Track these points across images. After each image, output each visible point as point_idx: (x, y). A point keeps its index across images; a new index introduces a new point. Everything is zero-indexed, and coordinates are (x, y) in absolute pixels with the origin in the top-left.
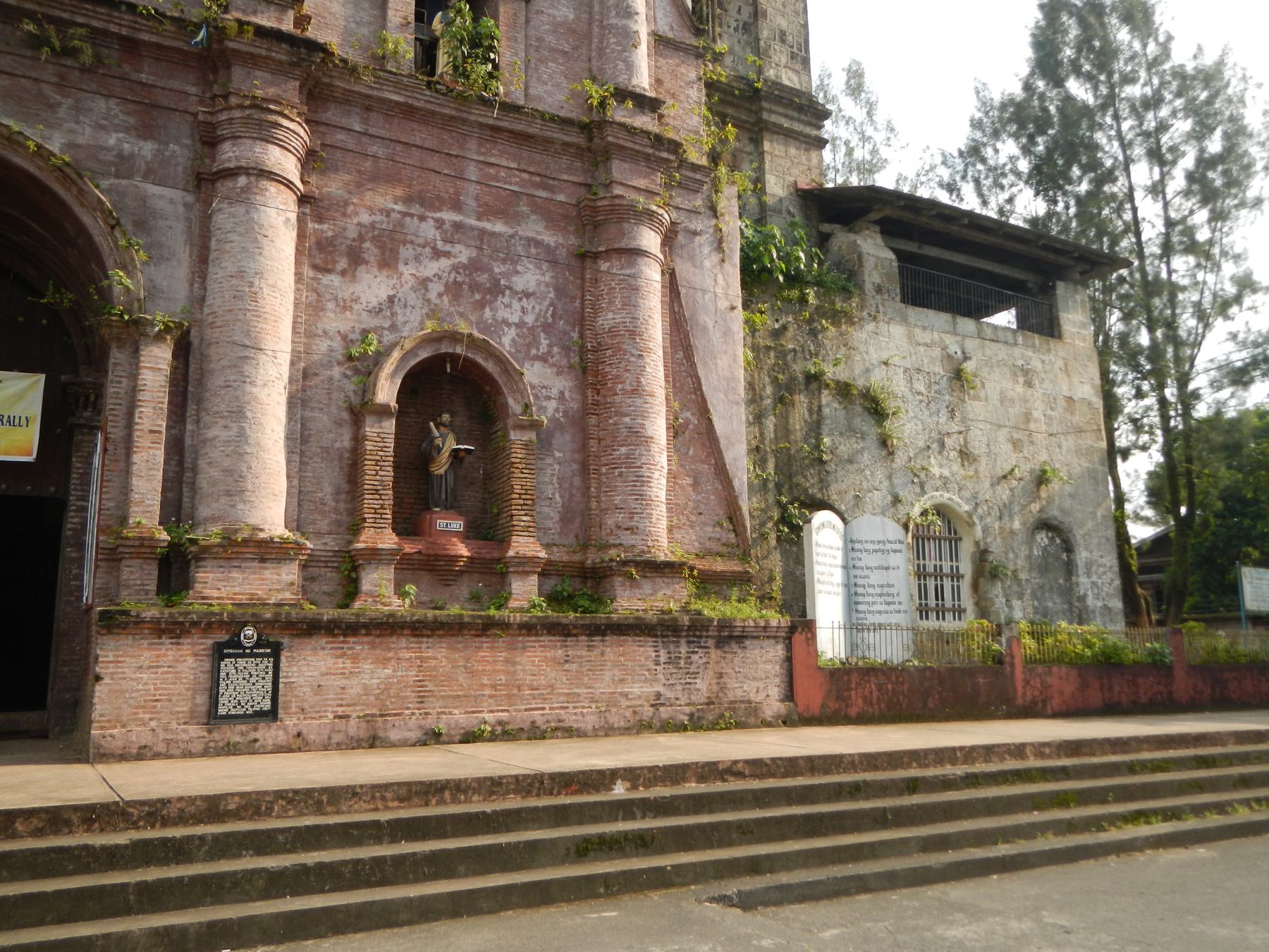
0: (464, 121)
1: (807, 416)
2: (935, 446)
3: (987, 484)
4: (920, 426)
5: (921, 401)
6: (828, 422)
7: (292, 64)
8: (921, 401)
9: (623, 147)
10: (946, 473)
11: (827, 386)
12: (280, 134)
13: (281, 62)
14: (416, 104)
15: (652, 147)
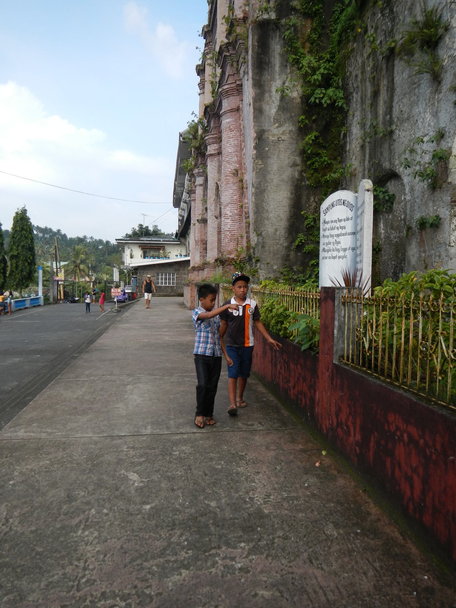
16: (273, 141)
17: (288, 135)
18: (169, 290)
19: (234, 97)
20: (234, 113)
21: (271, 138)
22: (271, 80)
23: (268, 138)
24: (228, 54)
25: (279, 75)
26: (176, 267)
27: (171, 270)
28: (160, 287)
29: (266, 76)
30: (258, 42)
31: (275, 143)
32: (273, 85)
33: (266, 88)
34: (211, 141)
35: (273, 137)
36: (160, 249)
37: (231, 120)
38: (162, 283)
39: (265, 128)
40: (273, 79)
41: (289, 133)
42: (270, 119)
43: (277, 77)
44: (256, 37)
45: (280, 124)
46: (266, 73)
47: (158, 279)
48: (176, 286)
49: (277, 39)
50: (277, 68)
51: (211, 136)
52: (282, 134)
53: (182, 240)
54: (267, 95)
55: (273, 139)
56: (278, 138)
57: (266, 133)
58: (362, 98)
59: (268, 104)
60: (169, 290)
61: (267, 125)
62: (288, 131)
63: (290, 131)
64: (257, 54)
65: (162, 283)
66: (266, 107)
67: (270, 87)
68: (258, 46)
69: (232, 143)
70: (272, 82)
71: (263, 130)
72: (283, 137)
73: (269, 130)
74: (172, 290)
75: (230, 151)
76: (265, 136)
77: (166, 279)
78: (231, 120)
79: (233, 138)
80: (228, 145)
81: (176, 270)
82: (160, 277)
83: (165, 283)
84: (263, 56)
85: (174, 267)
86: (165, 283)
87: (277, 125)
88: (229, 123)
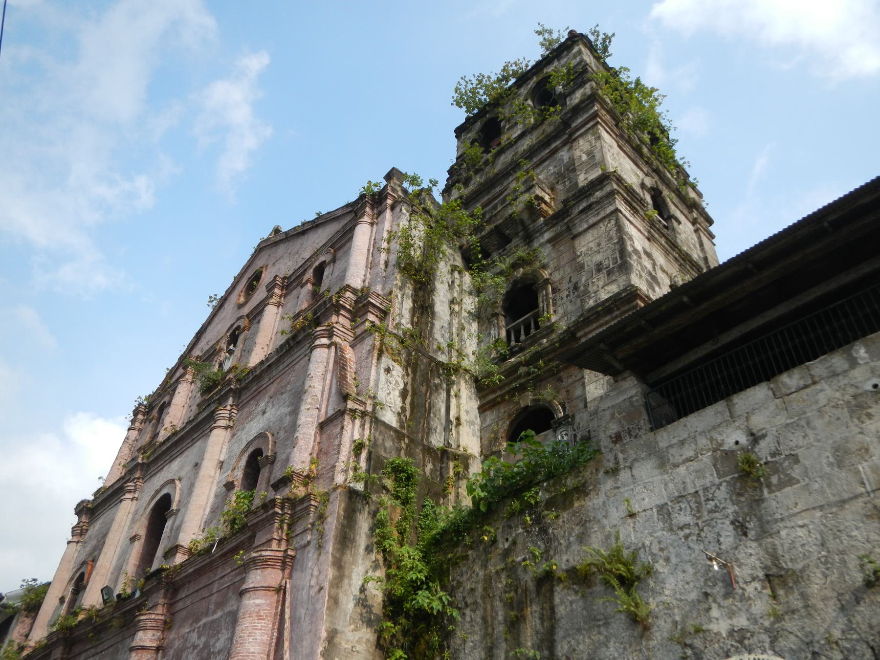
0: (214, 561)
1: (539, 626)
2: (718, 590)
3: (831, 611)
4: (691, 570)
5: (686, 537)
6: (563, 622)
7: (158, 583)
8: (686, 537)
9: (257, 523)
10: (742, 621)
11: (560, 580)
12: (141, 624)
13: (156, 585)
14: (197, 567)
15: (265, 512)
16: (345, 649)
17: (364, 645)
19: (275, 570)
20: (270, 593)
21: (344, 645)
22: (353, 564)
23: (340, 643)
24: (280, 511)
25: (363, 559)
29: (348, 557)
30: (345, 512)
31: (348, 653)
32: (355, 570)
33: (347, 573)
34: (154, 624)
35: (346, 644)
37: (263, 601)
39: (339, 628)
40: (354, 563)
41: (366, 643)
42: (346, 615)
43: (360, 562)
44: (343, 505)
45: (357, 627)
46: (348, 552)
49: (366, 515)
50: (362, 550)
51: (153, 616)
52: (357, 641)
54: (346, 581)
55: (346, 646)
56: (353, 647)
57: (338, 635)
58: (484, 619)
59: (346, 595)
61: (341, 623)
62: (364, 640)
63: (368, 640)
64: (342, 526)
66: (343, 598)
67: (351, 572)
68: (344, 517)
69: (259, 638)
70: (353, 567)
71: (336, 630)
72: (359, 648)
73: (343, 632)
75: (252, 650)
76: (336, 640)
78: (263, 601)
79: (261, 629)
80: (251, 640)
84: (348, 530)
87: (352, 627)
88: (258, 605)
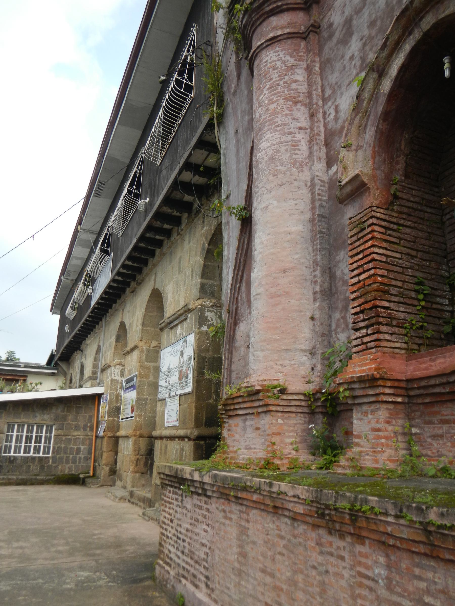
18: (34, 468)
26: (59, 411)
27: (46, 417)
28: (12, 460)
36: (17, 381)
38: (17, 450)
47: (9, 439)
48: (53, 457)
53: (63, 366)
60: (34, 468)
65: (17, 450)
74: (42, 467)
77: (29, 439)
81: (56, 419)
82: (15, 434)
83: (27, 450)
85: (54, 411)
86: (27, 450)
